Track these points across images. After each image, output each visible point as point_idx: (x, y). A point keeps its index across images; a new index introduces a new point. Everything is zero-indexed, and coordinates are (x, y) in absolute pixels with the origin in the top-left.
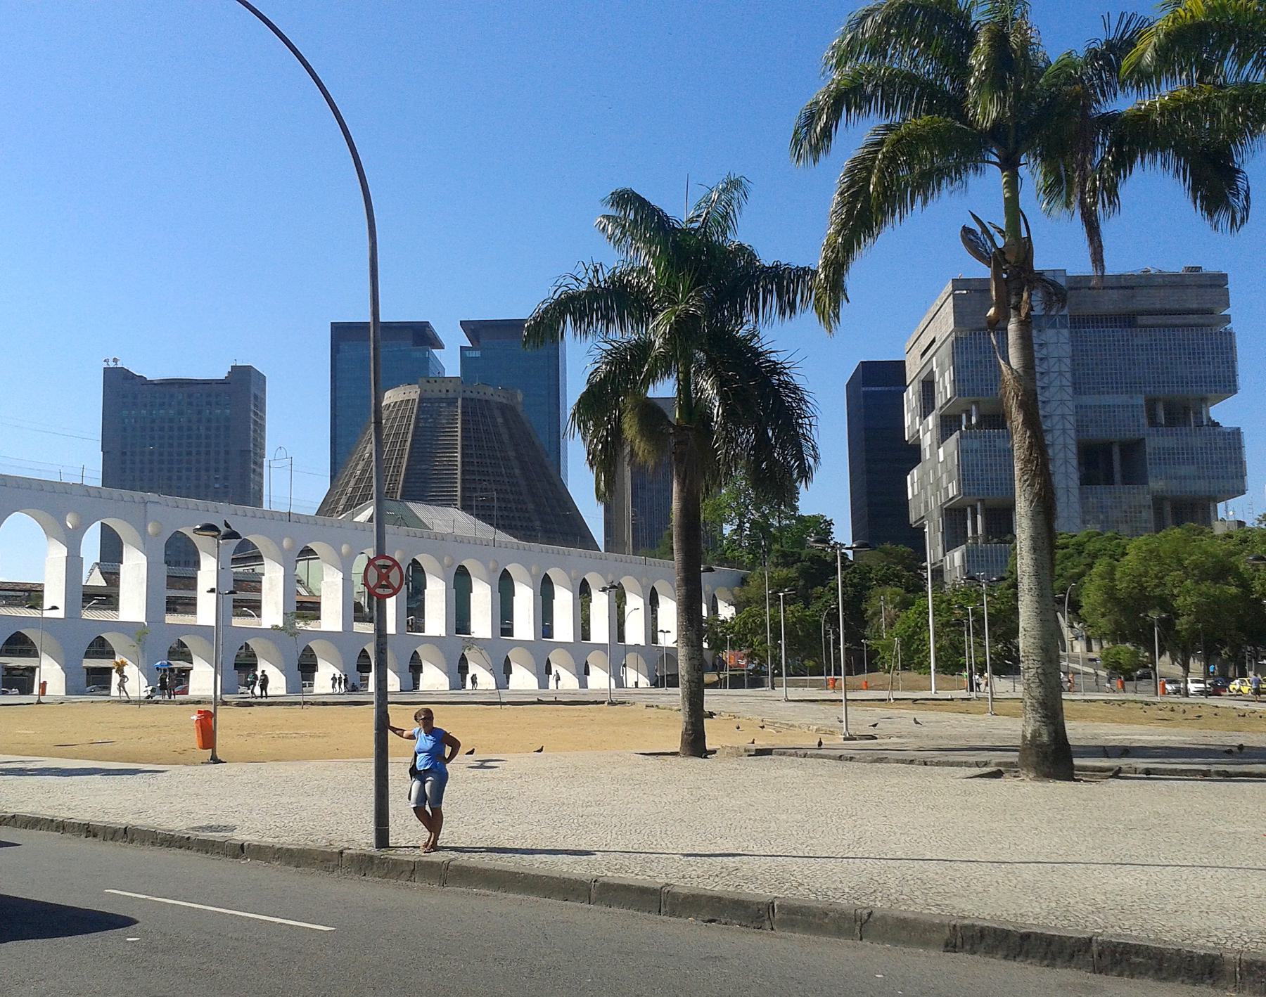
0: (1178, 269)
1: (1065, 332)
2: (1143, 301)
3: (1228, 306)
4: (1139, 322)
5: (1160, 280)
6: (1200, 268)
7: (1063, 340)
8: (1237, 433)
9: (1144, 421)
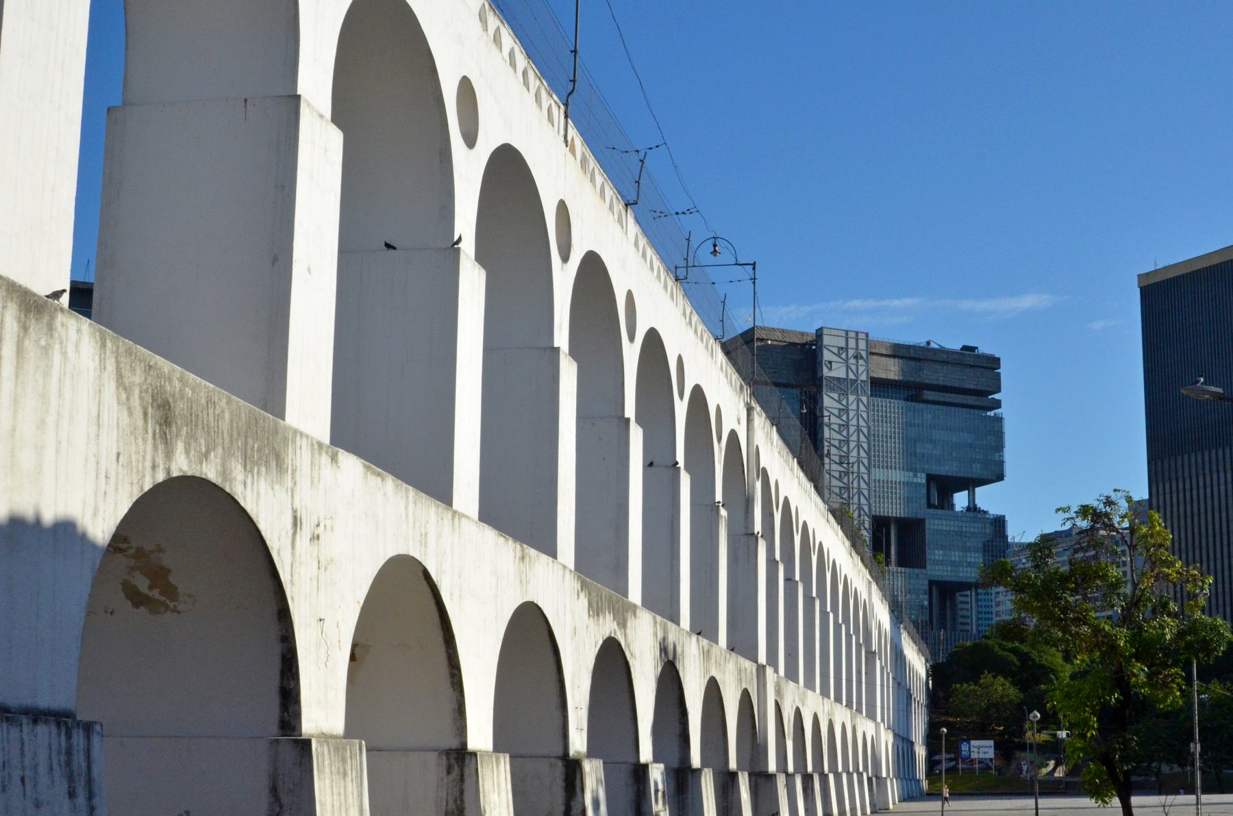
5: (944, 356)
6: (977, 348)
9: (924, 501)
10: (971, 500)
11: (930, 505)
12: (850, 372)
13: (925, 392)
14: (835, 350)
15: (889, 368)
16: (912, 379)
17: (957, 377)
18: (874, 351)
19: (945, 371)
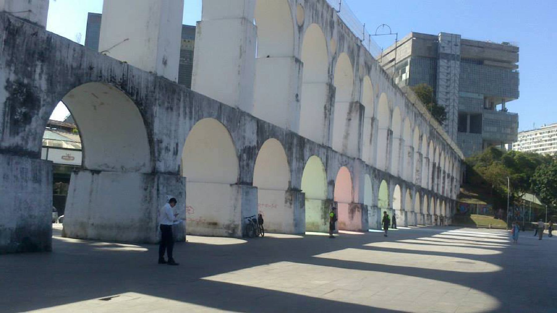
0: (500, 42)
1: (458, 63)
2: (487, 54)
3: (518, 61)
7: (457, 66)
8: (515, 116)
9: (482, 106)
11: (485, 108)
14: (447, 42)
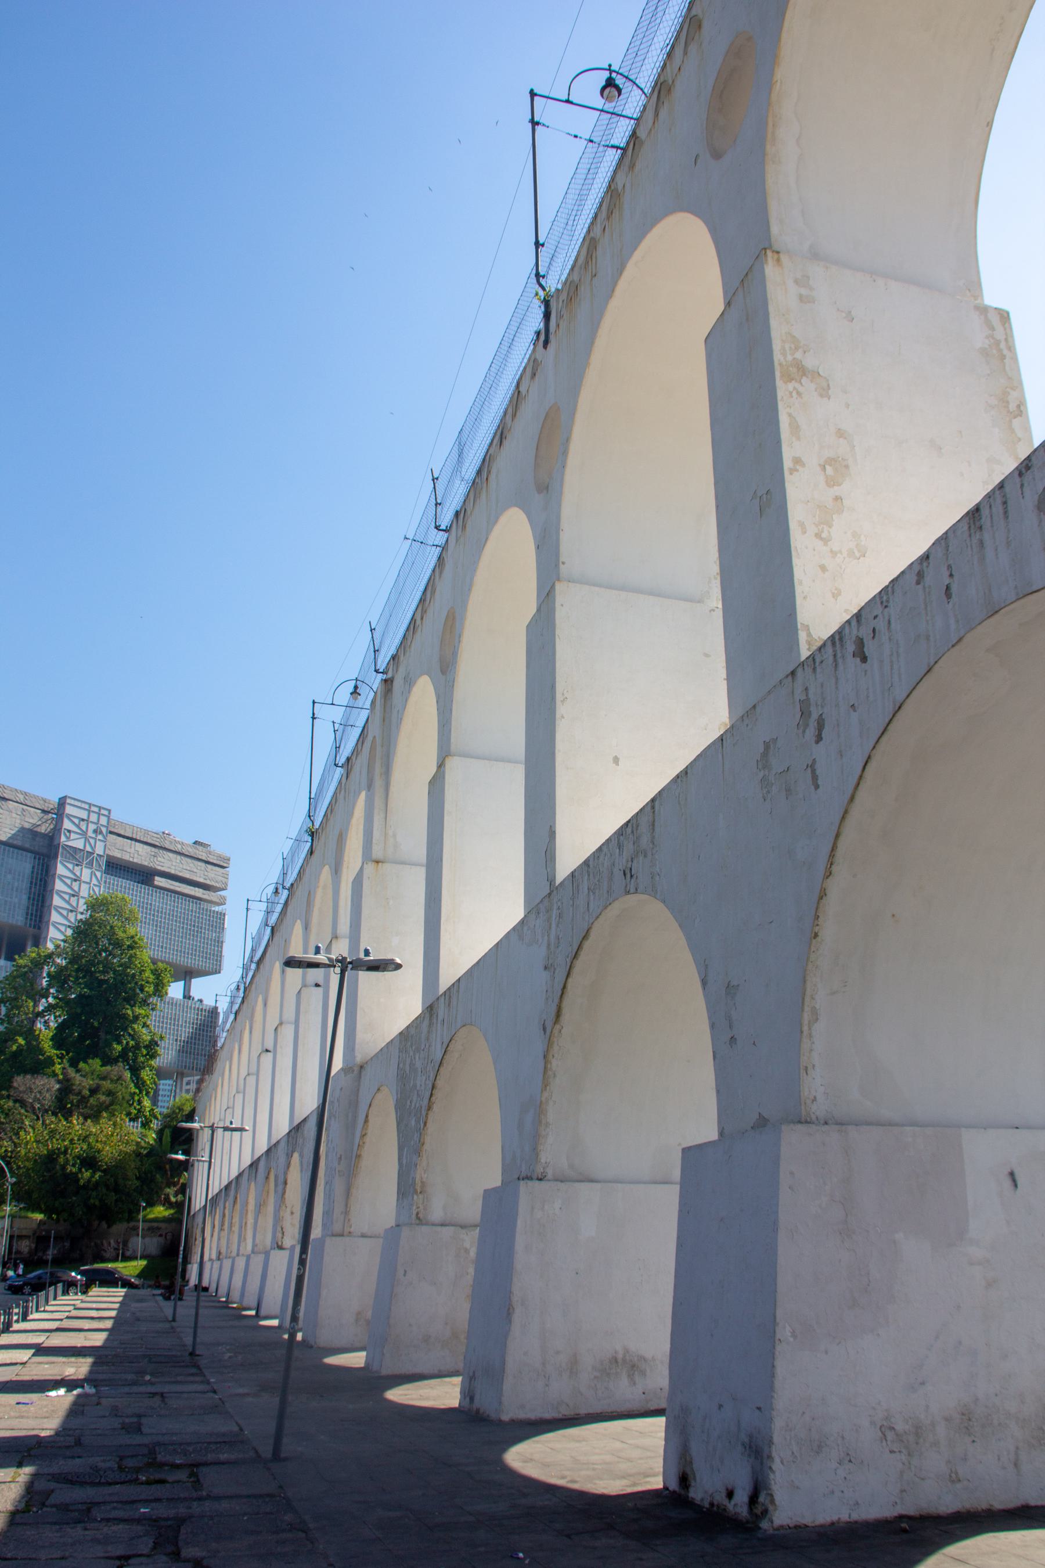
1: (99, 874)
4: (156, 883)
5: (179, 847)
10: (187, 988)
12: (87, 845)
13: (157, 878)
15: (125, 849)
16: (146, 864)
17: (189, 868)
18: (113, 830)
19: (178, 861)
